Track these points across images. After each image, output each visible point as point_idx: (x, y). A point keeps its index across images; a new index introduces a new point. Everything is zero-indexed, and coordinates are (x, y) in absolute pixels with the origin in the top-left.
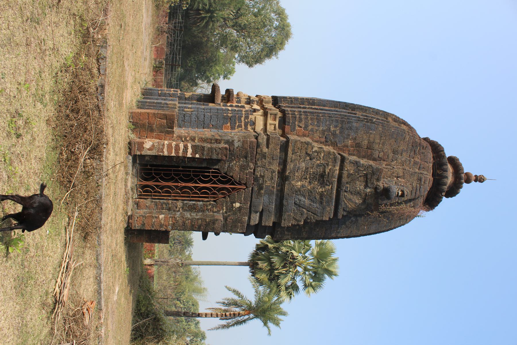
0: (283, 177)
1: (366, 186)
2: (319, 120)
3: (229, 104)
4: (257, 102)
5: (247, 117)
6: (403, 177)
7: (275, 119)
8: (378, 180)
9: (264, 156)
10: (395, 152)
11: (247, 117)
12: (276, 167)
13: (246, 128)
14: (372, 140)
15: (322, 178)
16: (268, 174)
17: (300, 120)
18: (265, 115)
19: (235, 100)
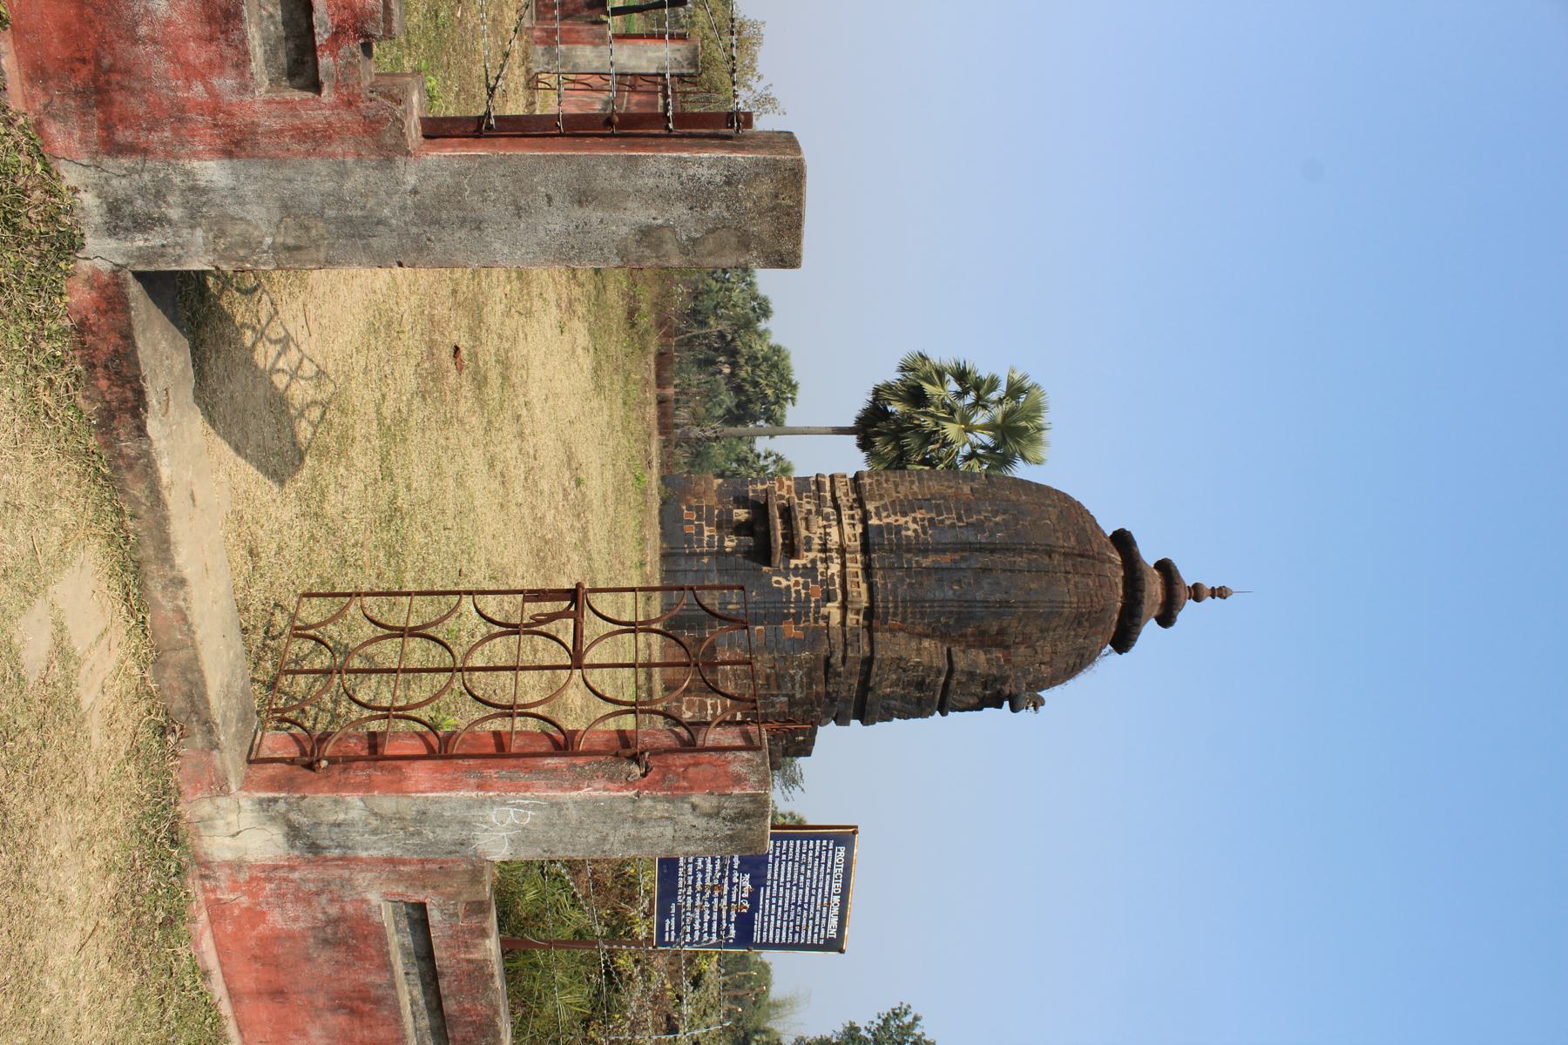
0: (865, 687)
1: (985, 688)
2: (923, 615)
3: (793, 562)
4: (837, 551)
5: (817, 612)
6: (1050, 664)
7: (858, 613)
8: (1003, 684)
9: (839, 675)
10: (1042, 631)
11: (817, 612)
12: (855, 682)
13: (816, 620)
14: (1005, 624)
15: (920, 685)
16: (843, 688)
17: (895, 614)
18: (844, 608)
19: (803, 547)
